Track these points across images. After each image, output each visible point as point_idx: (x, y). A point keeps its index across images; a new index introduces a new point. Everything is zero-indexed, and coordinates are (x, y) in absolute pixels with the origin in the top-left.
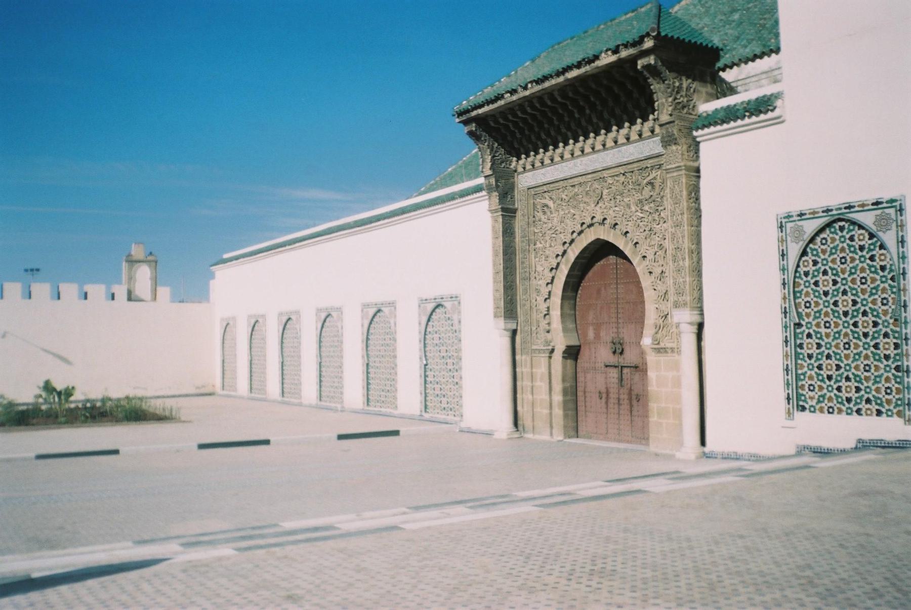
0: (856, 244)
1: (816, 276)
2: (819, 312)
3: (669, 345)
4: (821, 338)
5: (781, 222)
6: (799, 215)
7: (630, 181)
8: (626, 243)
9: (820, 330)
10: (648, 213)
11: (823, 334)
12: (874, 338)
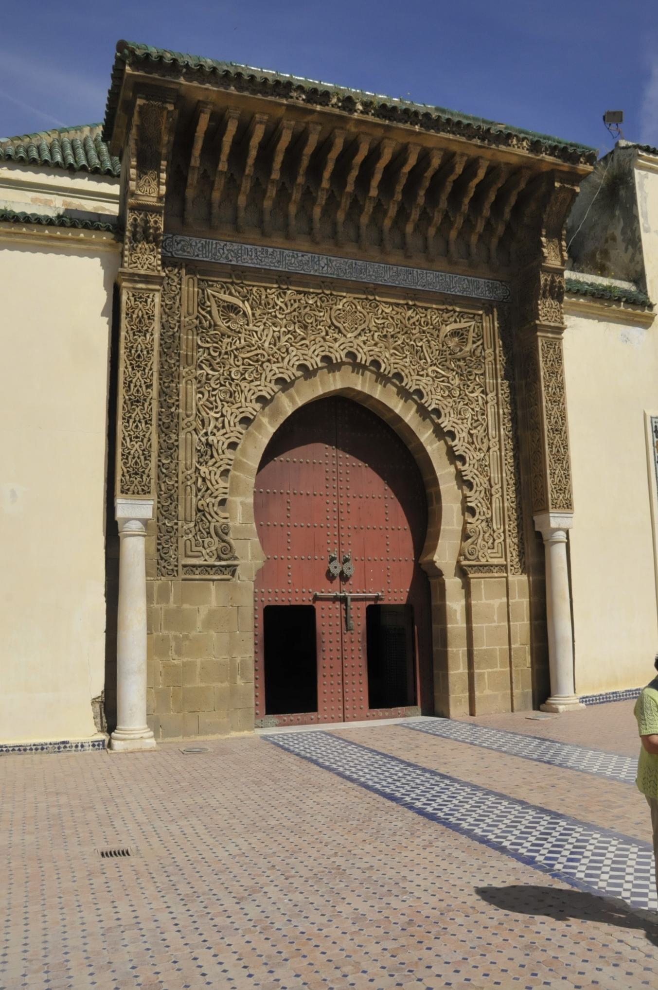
3: (495, 561)
7: (423, 320)
10: (454, 373)
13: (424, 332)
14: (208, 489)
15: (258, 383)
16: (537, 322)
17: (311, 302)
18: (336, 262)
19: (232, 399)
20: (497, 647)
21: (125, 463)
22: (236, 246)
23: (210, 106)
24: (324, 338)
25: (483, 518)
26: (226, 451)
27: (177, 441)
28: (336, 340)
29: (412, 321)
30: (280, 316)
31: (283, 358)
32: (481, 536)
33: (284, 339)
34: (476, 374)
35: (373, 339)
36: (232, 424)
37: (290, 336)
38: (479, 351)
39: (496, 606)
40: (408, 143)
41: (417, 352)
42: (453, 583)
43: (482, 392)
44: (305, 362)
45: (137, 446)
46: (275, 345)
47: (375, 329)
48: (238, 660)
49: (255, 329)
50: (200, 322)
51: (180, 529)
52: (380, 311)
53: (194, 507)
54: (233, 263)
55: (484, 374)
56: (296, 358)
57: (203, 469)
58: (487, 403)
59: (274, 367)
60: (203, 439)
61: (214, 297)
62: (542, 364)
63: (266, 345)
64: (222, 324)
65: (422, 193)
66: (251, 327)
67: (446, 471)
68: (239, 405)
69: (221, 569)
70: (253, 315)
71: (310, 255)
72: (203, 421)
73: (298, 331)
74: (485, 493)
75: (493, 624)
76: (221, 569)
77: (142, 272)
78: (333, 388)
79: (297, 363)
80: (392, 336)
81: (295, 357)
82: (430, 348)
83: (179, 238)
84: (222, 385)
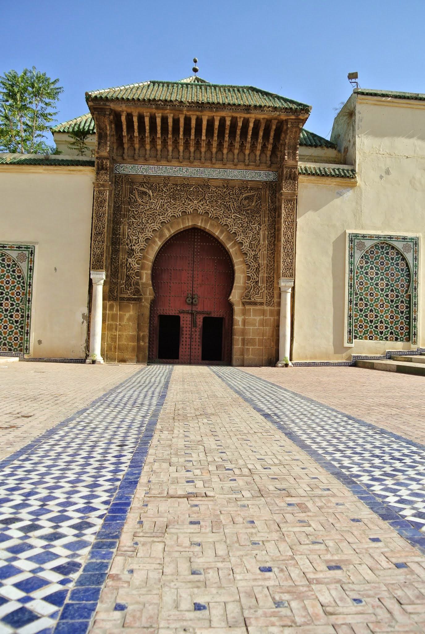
0: (390, 256)
1: (367, 269)
2: (368, 287)
3: (259, 300)
4: (368, 301)
5: (352, 238)
6: (362, 237)
8: (222, 232)
9: (367, 297)
11: (369, 299)
12: (396, 303)
13: (231, 198)
14: (131, 267)
15: (153, 224)
16: (283, 192)
17: (178, 188)
18: (190, 169)
19: (143, 231)
20: (257, 338)
21: (94, 258)
22: (146, 167)
23: (125, 112)
24: (183, 204)
25: (254, 281)
26: (139, 253)
27: (119, 248)
28: (189, 204)
29: (225, 194)
30: (164, 195)
31: (165, 213)
32: (253, 289)
33: (165, 205)
34: (256, 216)
35: (206, 203)
36: (142, 241)
37: (168, 204)
38: (259, 205)
39: (258, 320)
40: (214, 116)
41: (227, 208)
42: (238, 308)
43: (259, 224)
44: (174, 215)
45: (98, 251)
46: (162, 208)
47: (208, 198)
48: (142, 334)
49: (154, 201)
50: (131, 200)
51: (119, 283)
52: (210, 190)
53: (125, 274)
54: (145, 174)
55: (260, 216)
56: (170, 213)
57: (130, 260)
58: (261, 229)
59: (161, 217)
60: (130, 248)
61: (136, 189)
62: (283, 211)
63: (158, 208)
64: (140, 200)
65: (227, 136)
66: (152, 201)
67: (239, 260)
68: (145, 233)
69: (134, 299)
70: (153, 195)
71: (178, 167)
72: (130, 240)
73: (172, 201)
74: (256, 270)
75: (256, 328)
76: (134, 299)
77: (101, 183)
78: (187, 225)
79: (171, 215)
80: (216, 201)
81: (170, 213)
82: (234, 205)
83: (122, 165)
84: (138, 226)
